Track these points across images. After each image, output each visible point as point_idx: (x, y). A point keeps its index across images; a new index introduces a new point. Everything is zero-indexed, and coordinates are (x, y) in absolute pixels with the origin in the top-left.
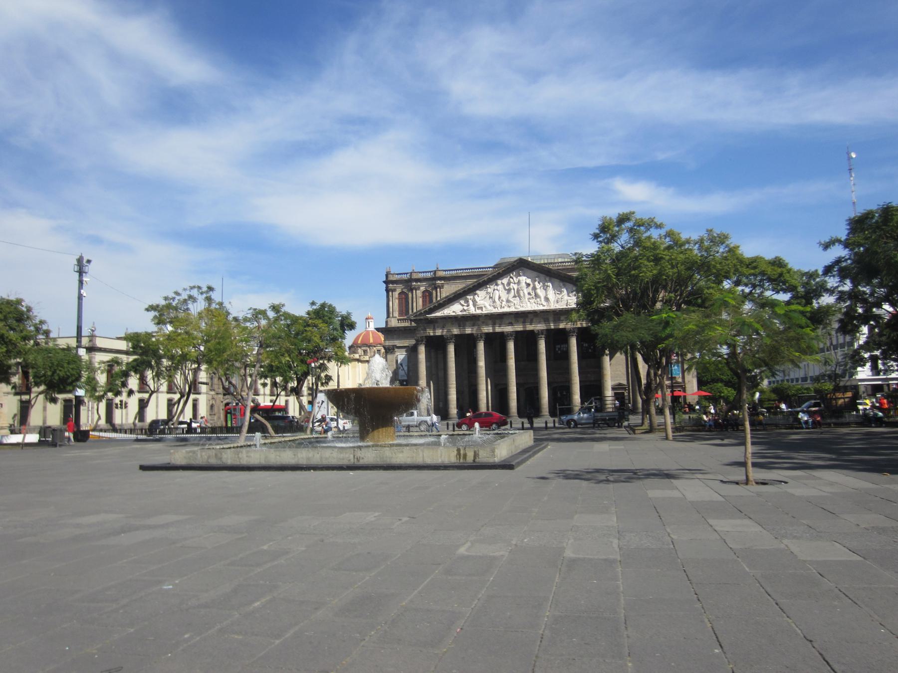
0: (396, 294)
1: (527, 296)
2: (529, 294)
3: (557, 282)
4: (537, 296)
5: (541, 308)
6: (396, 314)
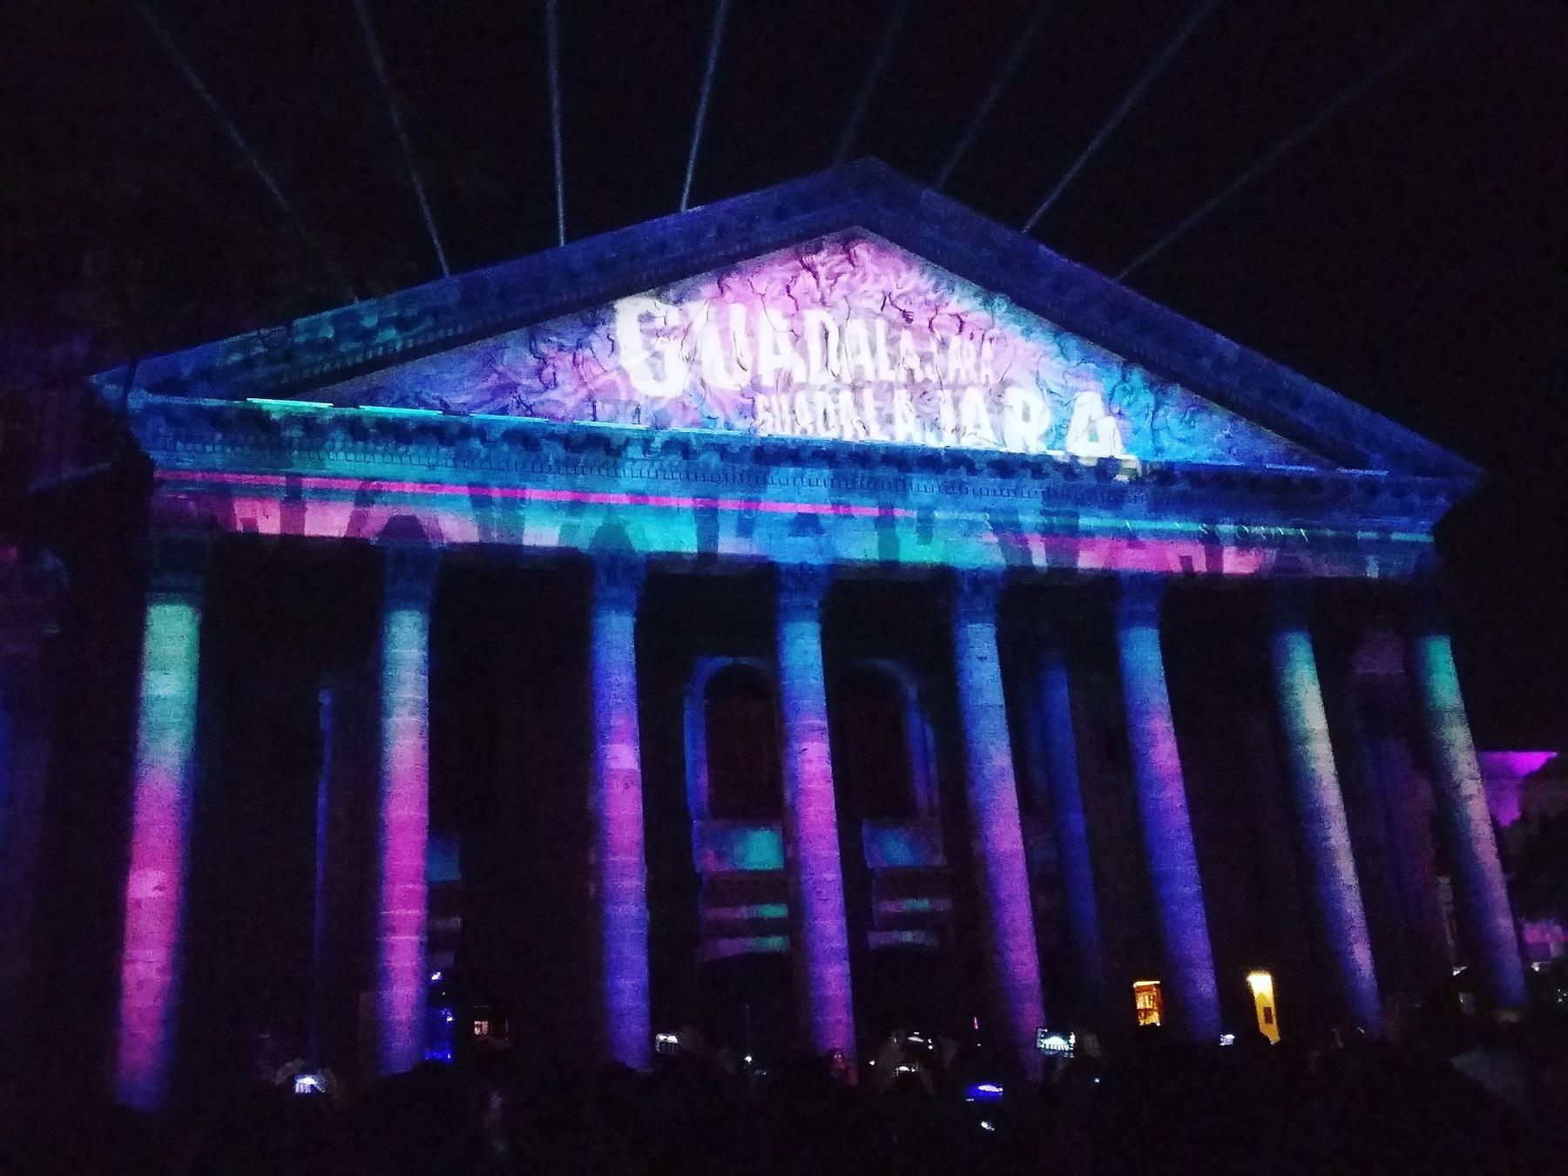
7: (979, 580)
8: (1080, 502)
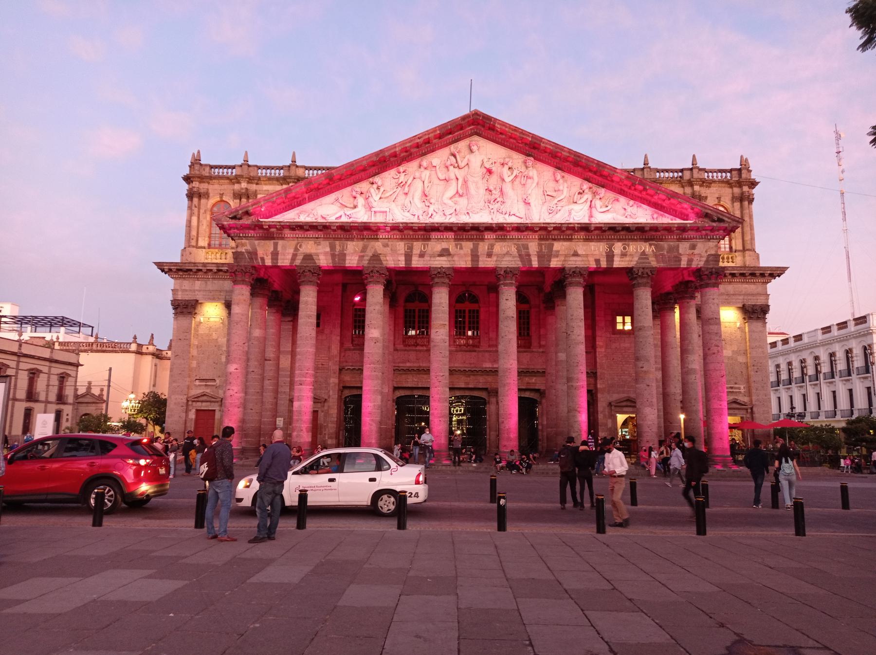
7: (509, 272)
8: (555, 240)
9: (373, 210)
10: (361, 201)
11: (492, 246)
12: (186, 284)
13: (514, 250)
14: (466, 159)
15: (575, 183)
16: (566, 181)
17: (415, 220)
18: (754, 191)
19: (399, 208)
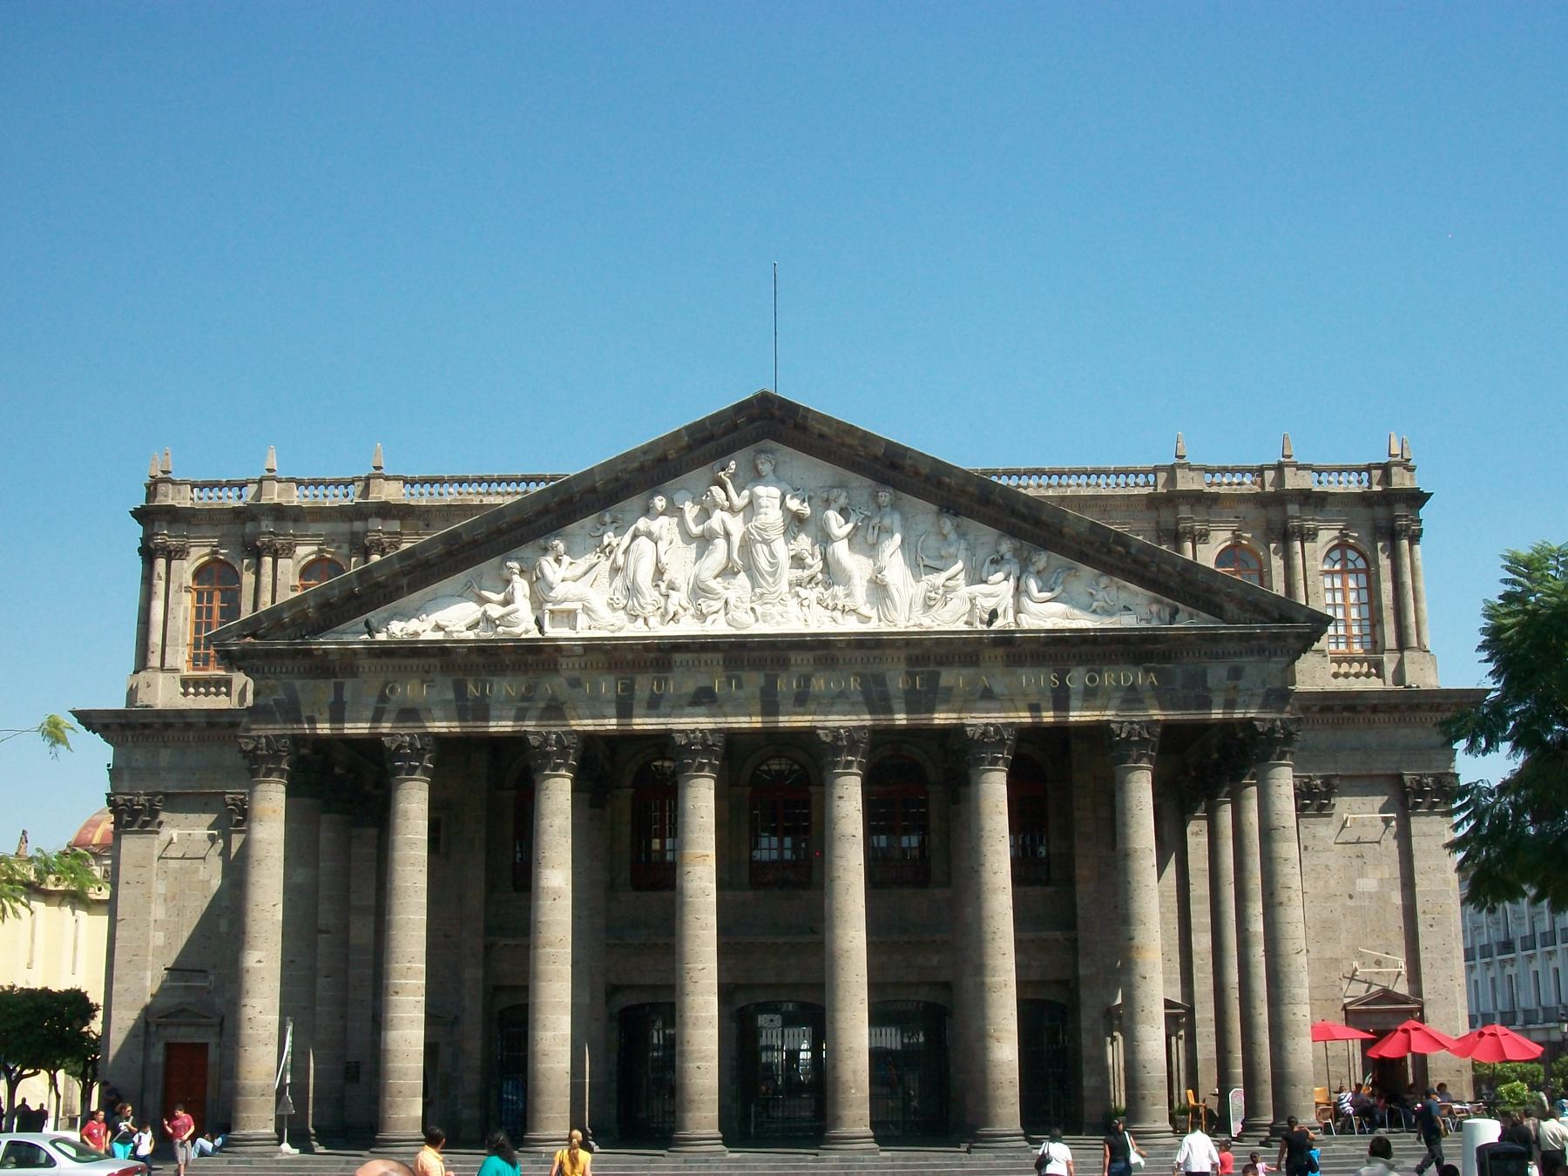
0: (185, 570)
1: (788, 574)
2: (798, 561)
3: (923, 511)
4: (831, 574)
5: (851, 625)
6: (180, 657)
9: (549, 606)
10: (520, 586)
11: (807, 679)
12: (140, 757)
13: (854, 684)
14: (746, 493)
15: (985, 539)
16: (962, 535)
17: (636, 630)
18: (1423, 513)
19: (606, 598)
